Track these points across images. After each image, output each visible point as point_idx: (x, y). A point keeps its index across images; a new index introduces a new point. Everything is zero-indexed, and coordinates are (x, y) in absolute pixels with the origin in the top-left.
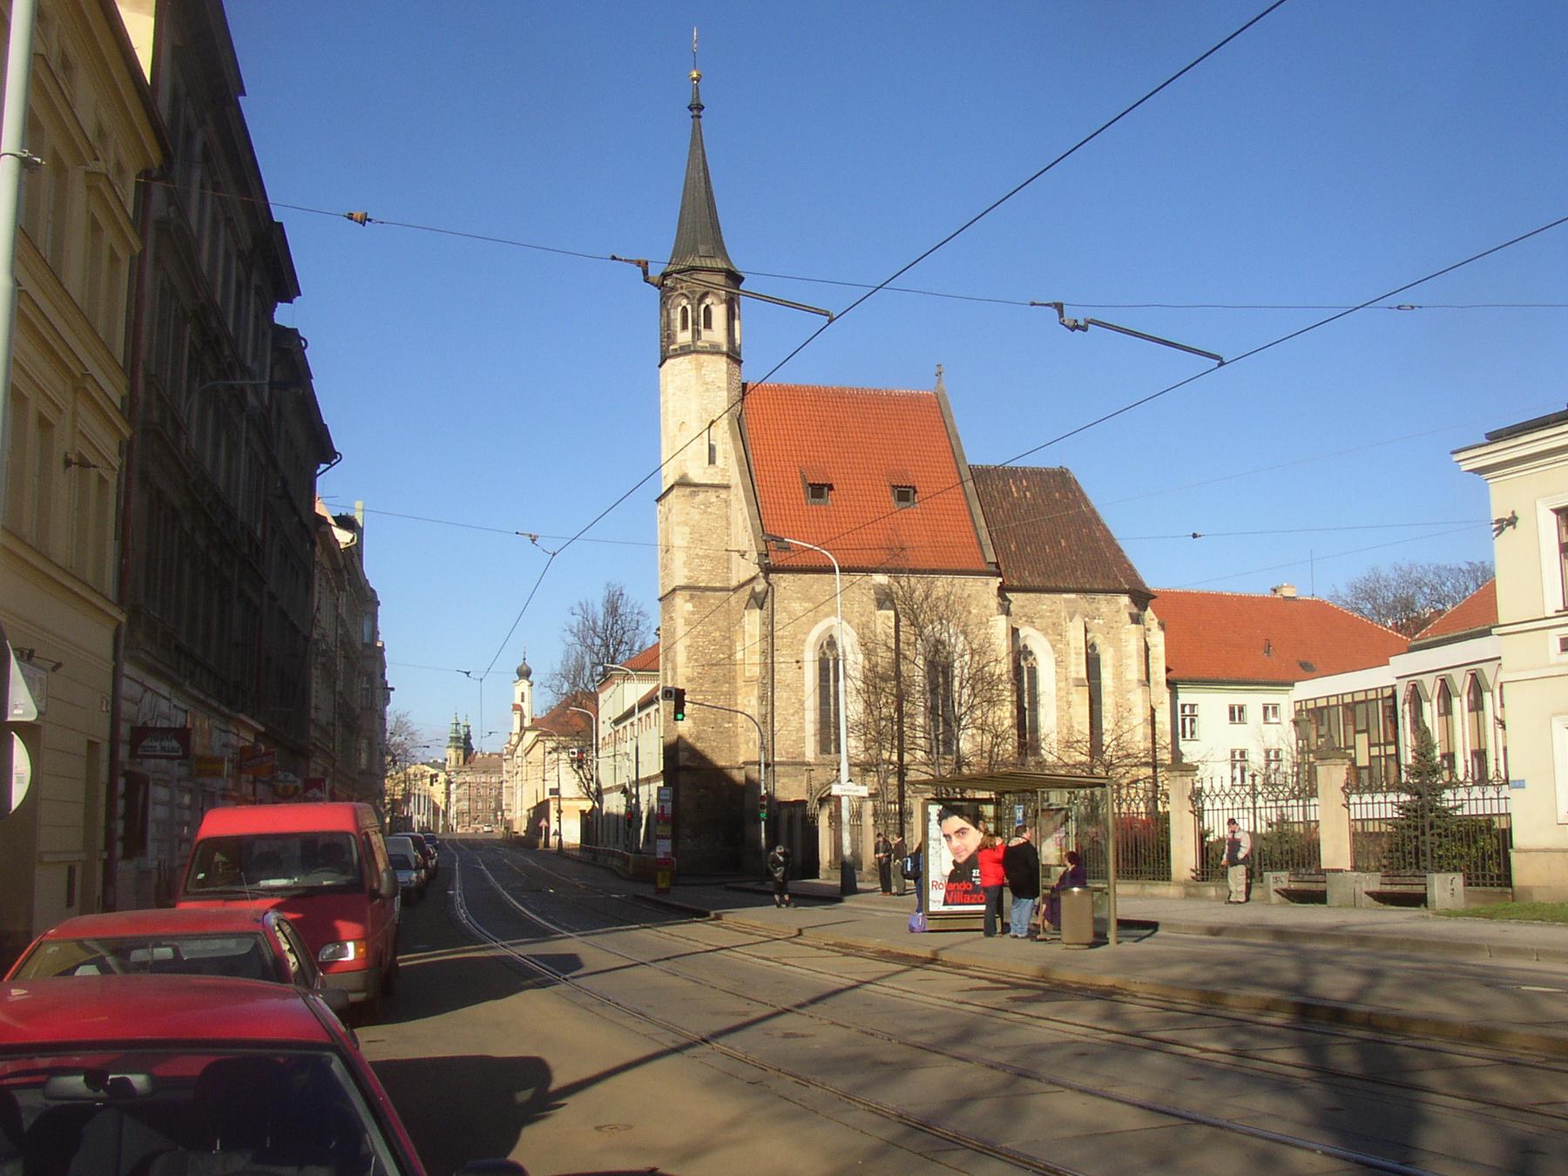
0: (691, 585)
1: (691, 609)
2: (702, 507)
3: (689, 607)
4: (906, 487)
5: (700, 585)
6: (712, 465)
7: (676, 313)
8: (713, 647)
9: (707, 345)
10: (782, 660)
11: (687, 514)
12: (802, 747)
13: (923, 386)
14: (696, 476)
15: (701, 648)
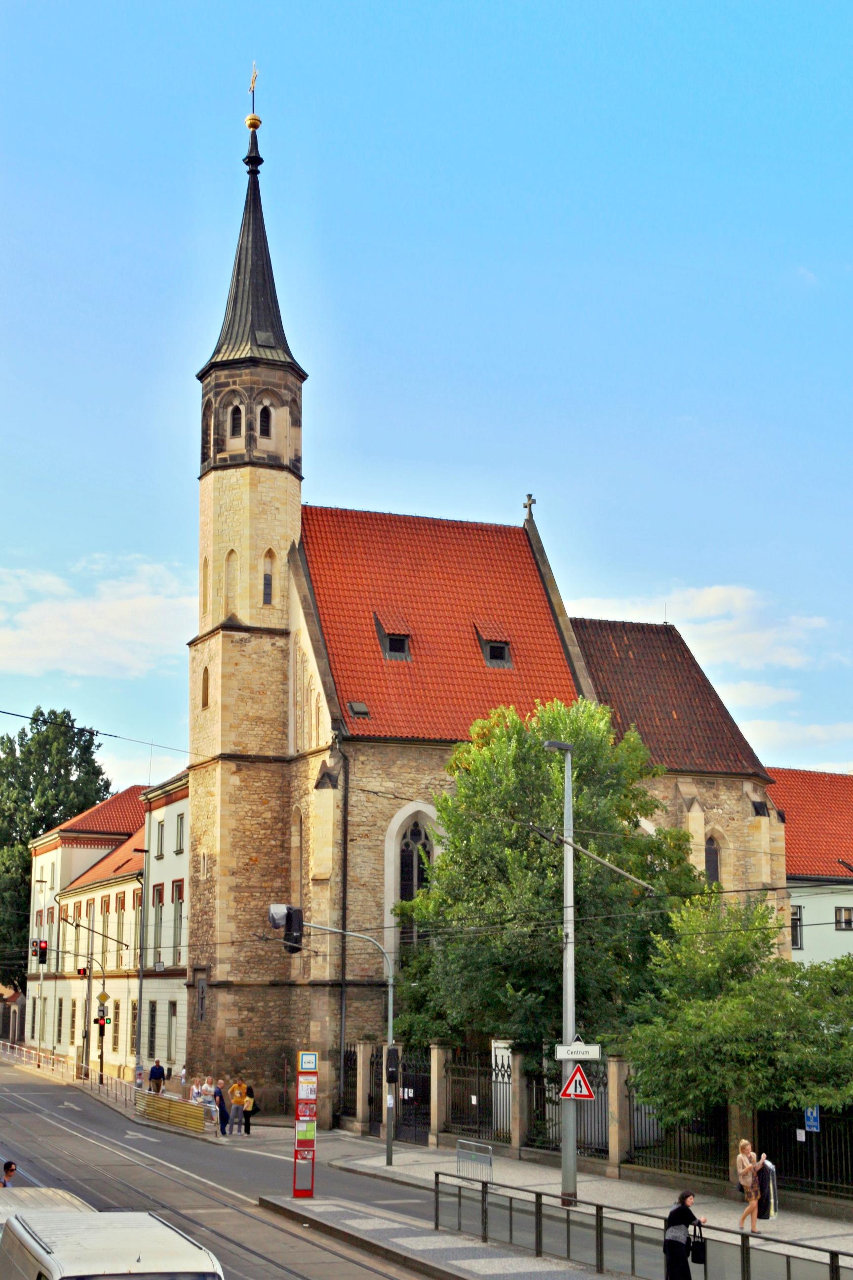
0: (239, 753)
2: (254, 656)
3: (236, 780)
4: (500, 642)
5: (249, 753)
6: (268, 607)
7: (225, 414)
9: (265, 456)
10: (358, 852)
11: (236, 664)
12: (380, 963)
13: (517, 520)
14: (245, 618)
15: (248, 833)
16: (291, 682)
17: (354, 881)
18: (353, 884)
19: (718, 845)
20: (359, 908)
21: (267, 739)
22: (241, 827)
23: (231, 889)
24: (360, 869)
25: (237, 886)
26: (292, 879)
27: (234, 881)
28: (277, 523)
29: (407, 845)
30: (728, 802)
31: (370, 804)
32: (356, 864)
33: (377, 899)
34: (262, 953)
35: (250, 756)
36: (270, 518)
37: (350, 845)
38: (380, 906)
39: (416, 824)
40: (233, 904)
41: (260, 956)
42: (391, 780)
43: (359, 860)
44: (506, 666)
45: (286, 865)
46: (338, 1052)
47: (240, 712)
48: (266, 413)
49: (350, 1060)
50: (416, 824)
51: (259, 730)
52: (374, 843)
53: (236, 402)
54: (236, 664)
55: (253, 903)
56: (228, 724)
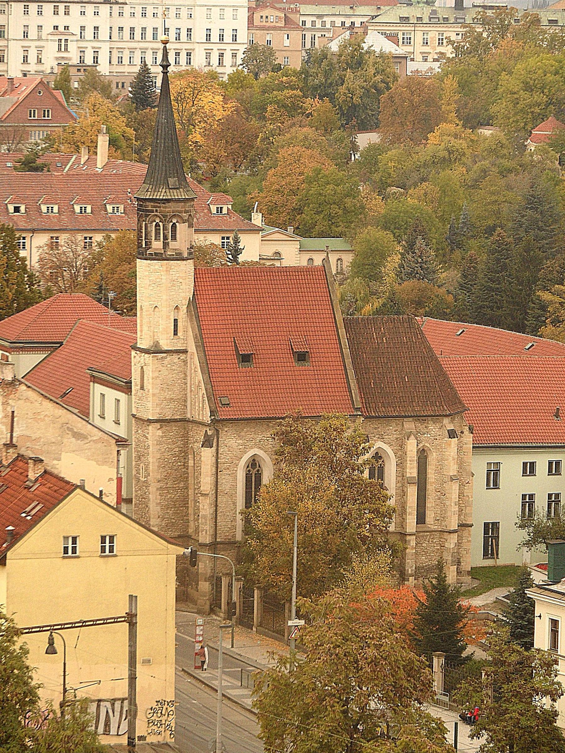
1: (161, 434)
3: (160, 433)
7: (151, 226)
11: (160, 371)
14: (165, 346)
16: (189, 378)
18: (221, 493)
19: (427, 454)
21: (176, 410)
23: (157, 489)
24: (224, 479)
26: (189, 482)
27: (159, 485)
28: (180, 291)
30: (434, 430)
34: (174, 521)
38: (234, 504)
39: (254, 460)
41: (173, 522)
44: (307, 366)
45: (186, 475)
46: (213, 576)
48: (174, 226)
49: (219, 580)
50: (254, 460)
51: (172, 406)
52: (232, 472)
53: (158, 220)
54: (160, 371)
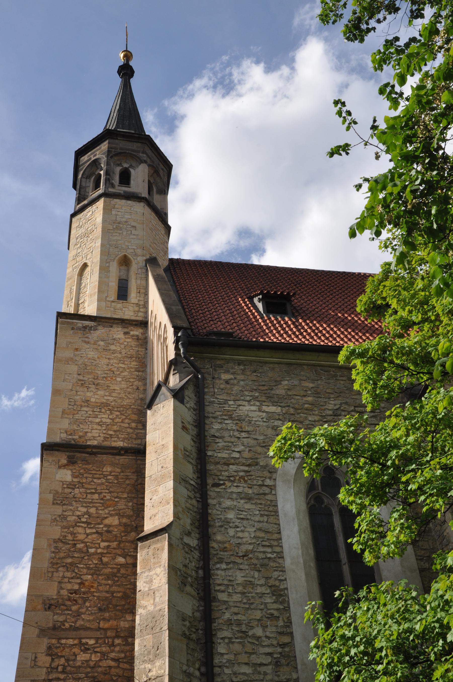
1: (69, 478)
2: (102, 343)
8: (103, 544)
10: (228, 503)
11: (77, 349)
15: (80, 546)
17: (224, 550)
20: (237, 597)
21: (115, 428)
22: (70, 537)
25: (55, 628)
29: (318, 499)
31: (243, 435)
32: (227, 522)
33: (271, 582)
35: (89, 446)
36: (124, 233)
37: (212, 492)
40: (45, 660)
42: (274, 404)
43: (231, 515)
47: (78, 398)
51: (105, 417)
54: (77, 349)
55: (82, 657)
56: (61, 410)
